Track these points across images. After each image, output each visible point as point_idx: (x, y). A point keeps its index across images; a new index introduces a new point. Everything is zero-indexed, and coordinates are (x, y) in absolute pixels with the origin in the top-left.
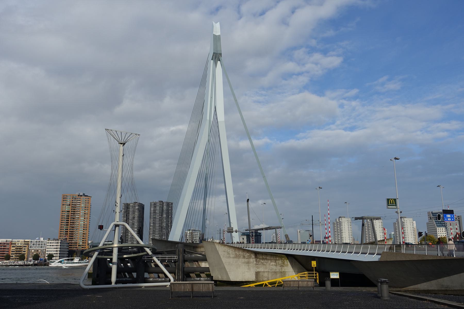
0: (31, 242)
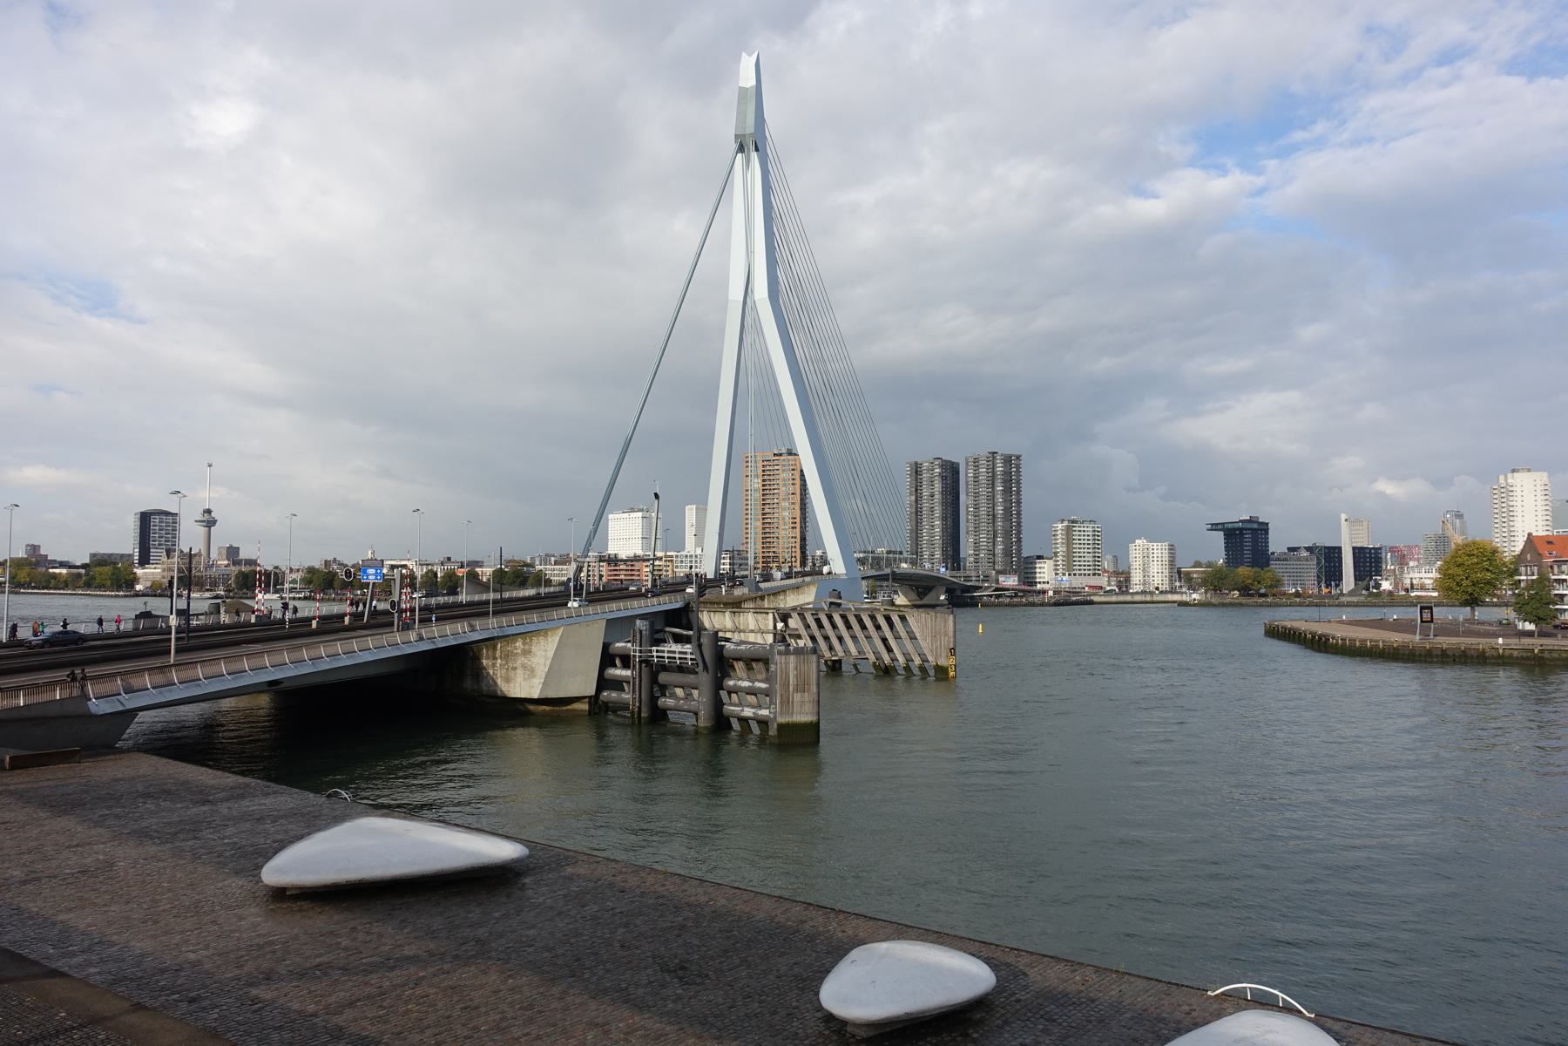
0: (677, 556)
